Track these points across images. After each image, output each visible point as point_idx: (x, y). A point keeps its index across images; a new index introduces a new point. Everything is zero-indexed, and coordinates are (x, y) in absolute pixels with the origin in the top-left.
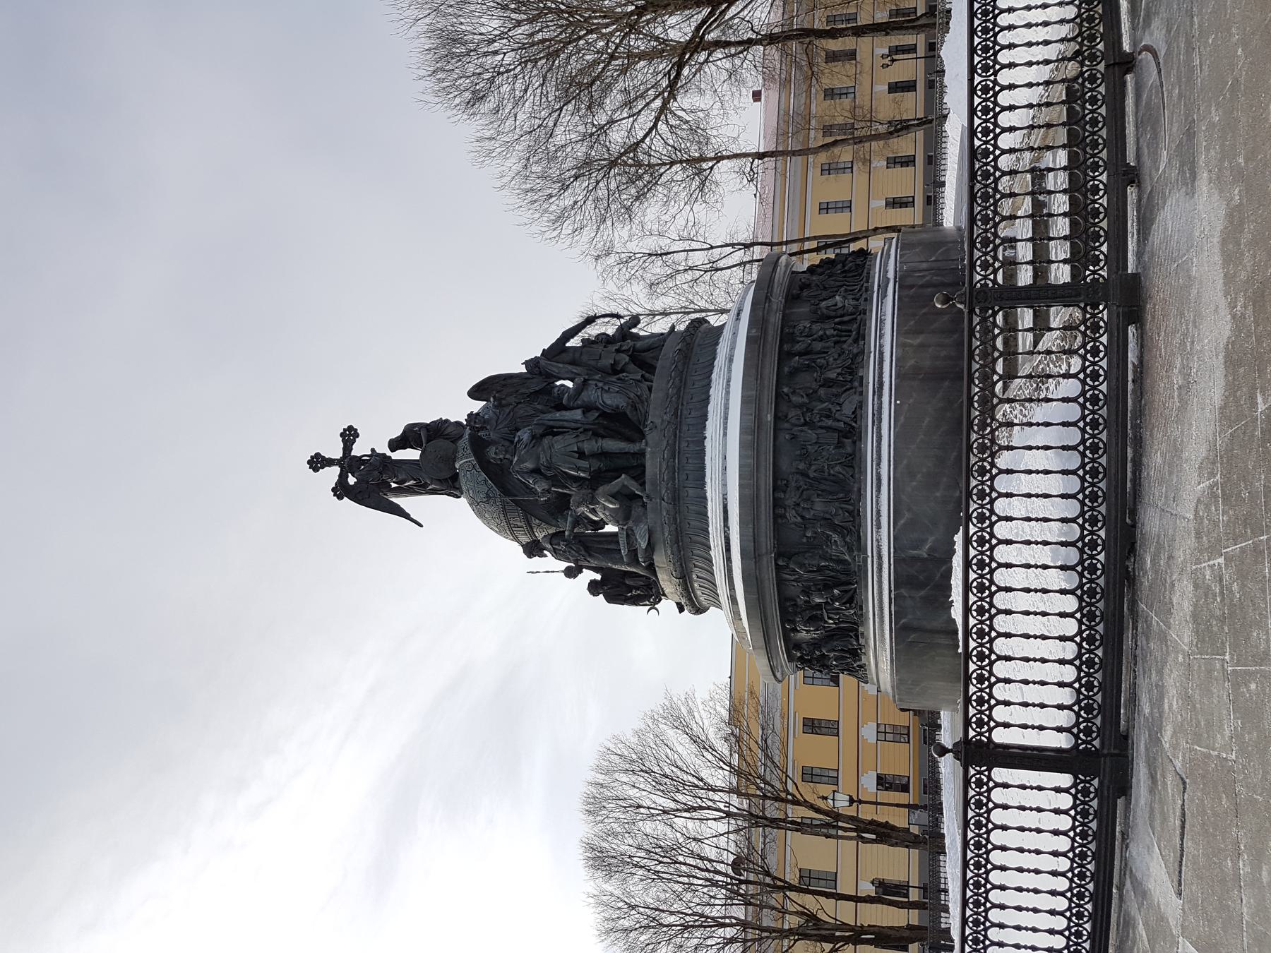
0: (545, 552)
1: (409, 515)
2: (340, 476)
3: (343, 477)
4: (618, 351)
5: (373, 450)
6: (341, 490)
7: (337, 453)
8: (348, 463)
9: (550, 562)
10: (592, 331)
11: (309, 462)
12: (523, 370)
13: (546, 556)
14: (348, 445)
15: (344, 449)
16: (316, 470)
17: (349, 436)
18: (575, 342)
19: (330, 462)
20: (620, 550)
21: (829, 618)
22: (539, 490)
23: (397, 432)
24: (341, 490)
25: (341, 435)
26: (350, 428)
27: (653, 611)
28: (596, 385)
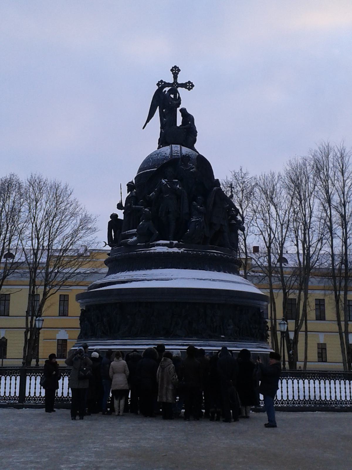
0: (130, 193)
2: (169, 83)
3: (168, 85)
6: (162, 85)
7: (181, 80)
8: (175, 86)
9: (126, 194)
11: (175, 67)
12: (216, 178)
13: (128, 193)
14: (184, 85)
15: (182, 84)
16: (172, 70)
17: (189, 86)
19: (175, 77)
21: (98, 324)
23: (189, 111)
24: (162, 85)
25: (189, 82)
26: (193, 86)
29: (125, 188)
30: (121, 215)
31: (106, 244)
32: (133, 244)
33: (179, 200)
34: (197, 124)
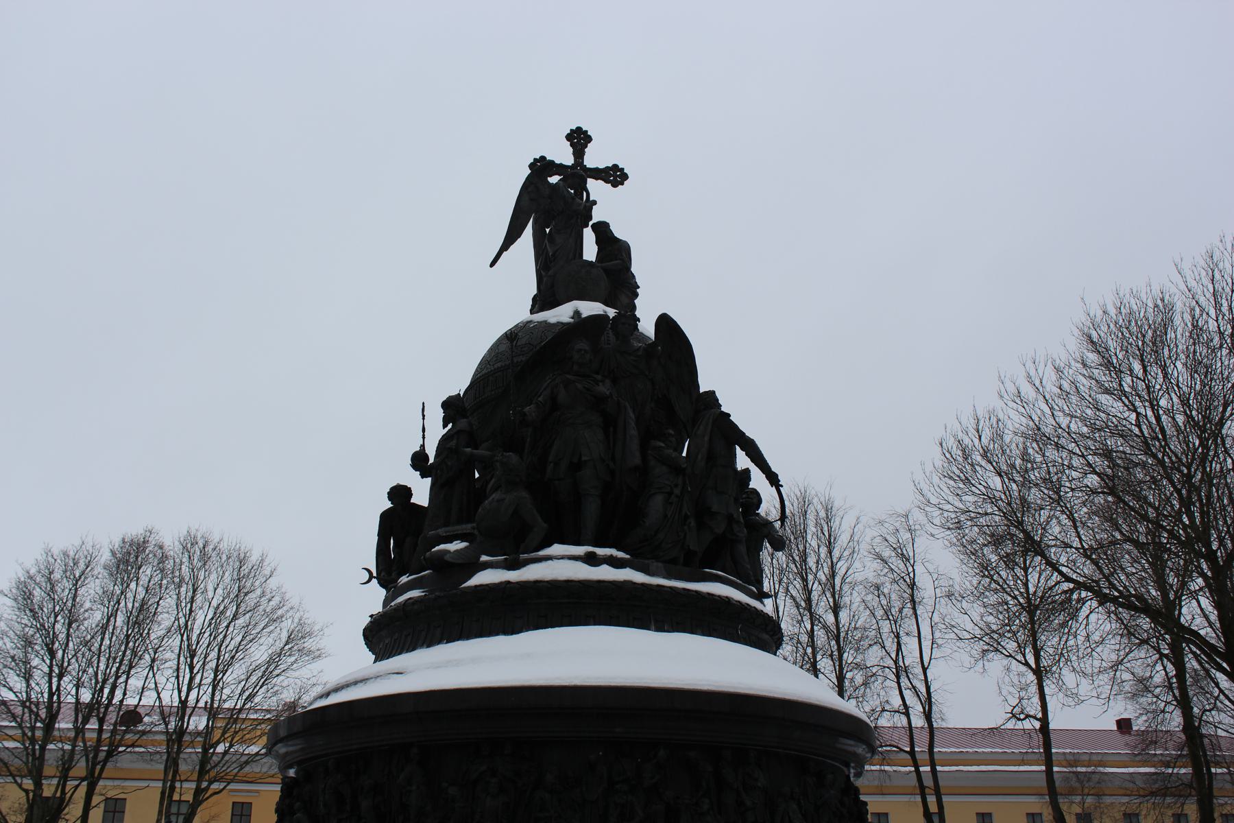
0: (450, 426)
1: (506, 251)
2: (561, 166)
4: (730, 519)
5: (595, 203)
6: (542, 167)
7: (593, 158)
8: (578, 175)
9: (437, 431)
10: (758, 481)
12: (704, 387)
13: (445, 426)
14: (599, 174)
16: (569, 137)
17: (615, 176)
18: (742, 461)
19: (579, 153)
20: (446, 524)
22: (527, 409)
23: (619, 232)
24: (542, 167)
25: (615, 167)
26: (624, 177)
27: (367, 576)
28: (676, 486)
29: (436, 415)
30: (422, 492)
31: (371, 577)
32: (460, 562)
33: (611, 429)
34: (639, 268)
